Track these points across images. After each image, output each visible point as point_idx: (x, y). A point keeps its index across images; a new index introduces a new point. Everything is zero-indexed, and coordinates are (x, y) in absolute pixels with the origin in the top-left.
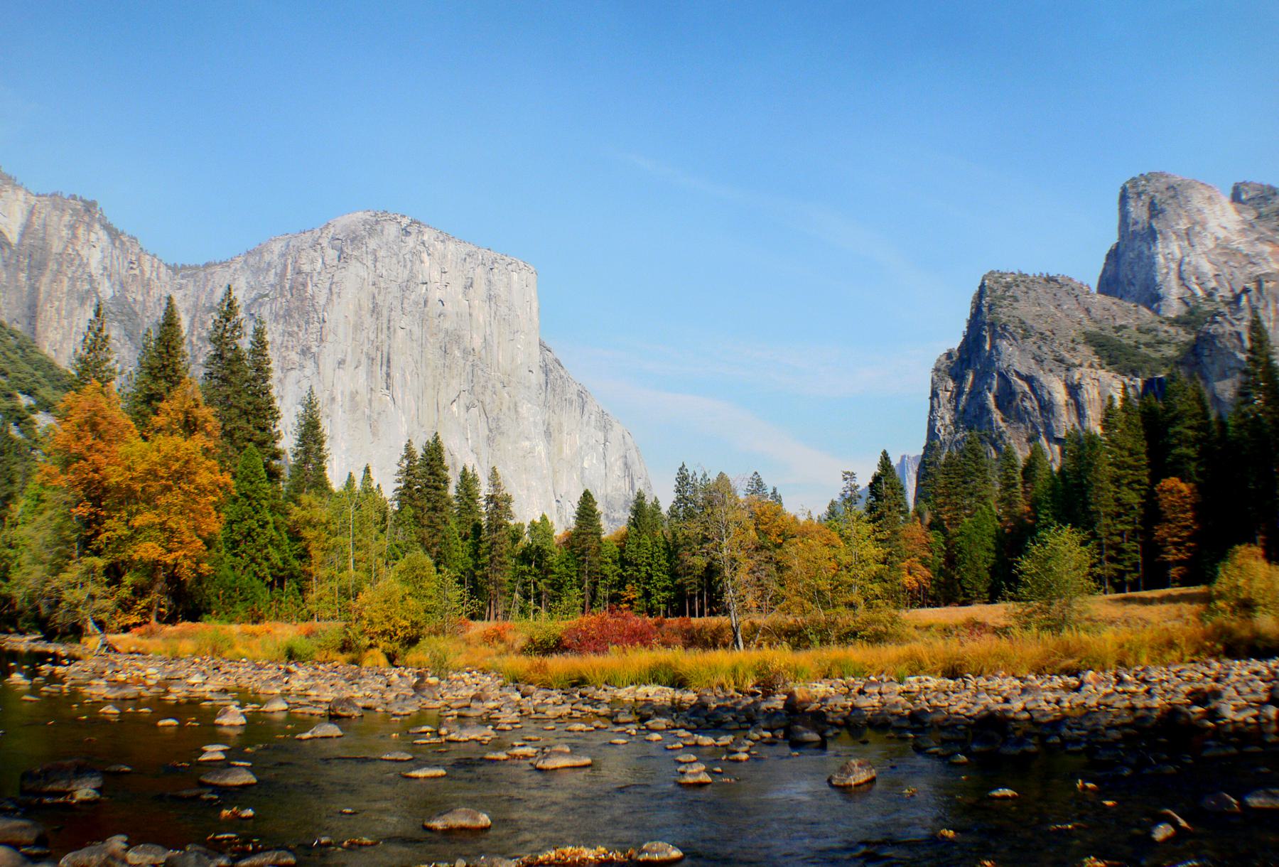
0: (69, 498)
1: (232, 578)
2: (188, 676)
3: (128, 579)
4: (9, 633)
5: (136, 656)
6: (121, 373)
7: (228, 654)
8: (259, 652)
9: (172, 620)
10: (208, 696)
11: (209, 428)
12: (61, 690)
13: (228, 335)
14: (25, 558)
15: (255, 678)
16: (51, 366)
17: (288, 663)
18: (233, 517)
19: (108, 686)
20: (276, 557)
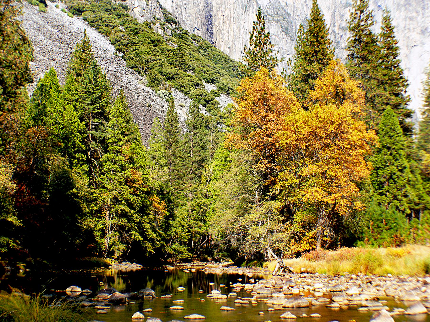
0: (250, 158)
1: (379, 212)
2: (347, 289)
3: (298, 217)
4: (208, 261)
5: (306, 275)
6: (282, 61)
7: (378, 271)
8: (402, 269)
9: (333, 246)
10: (364, 303)
11: (355, 96)
12: (250, 302)
13: (362, 23)
14: (218, 204)
15: (400, 288)
16: (227, 59)
17: (424, 277)
18: (378, 164)
19: (285, 298)
20: (412, 194)
